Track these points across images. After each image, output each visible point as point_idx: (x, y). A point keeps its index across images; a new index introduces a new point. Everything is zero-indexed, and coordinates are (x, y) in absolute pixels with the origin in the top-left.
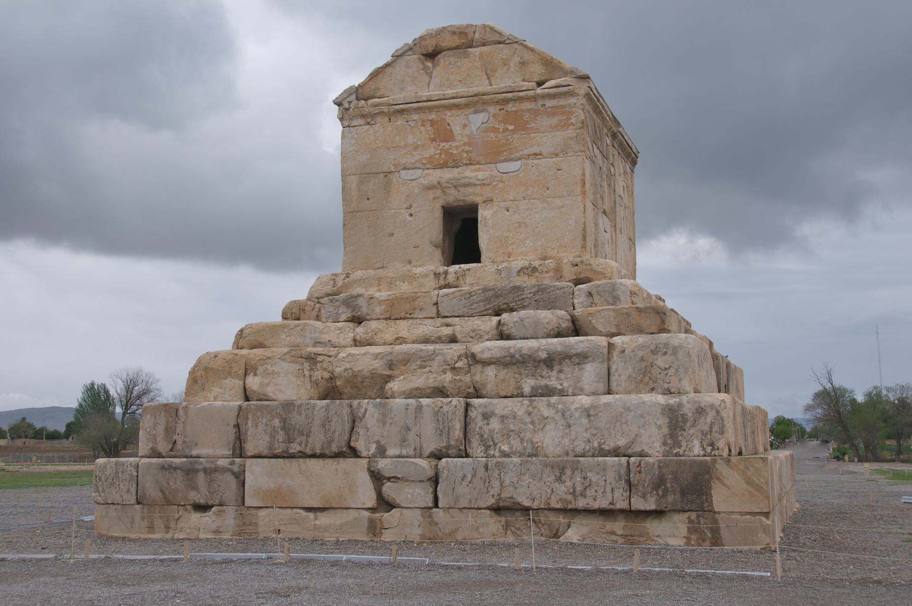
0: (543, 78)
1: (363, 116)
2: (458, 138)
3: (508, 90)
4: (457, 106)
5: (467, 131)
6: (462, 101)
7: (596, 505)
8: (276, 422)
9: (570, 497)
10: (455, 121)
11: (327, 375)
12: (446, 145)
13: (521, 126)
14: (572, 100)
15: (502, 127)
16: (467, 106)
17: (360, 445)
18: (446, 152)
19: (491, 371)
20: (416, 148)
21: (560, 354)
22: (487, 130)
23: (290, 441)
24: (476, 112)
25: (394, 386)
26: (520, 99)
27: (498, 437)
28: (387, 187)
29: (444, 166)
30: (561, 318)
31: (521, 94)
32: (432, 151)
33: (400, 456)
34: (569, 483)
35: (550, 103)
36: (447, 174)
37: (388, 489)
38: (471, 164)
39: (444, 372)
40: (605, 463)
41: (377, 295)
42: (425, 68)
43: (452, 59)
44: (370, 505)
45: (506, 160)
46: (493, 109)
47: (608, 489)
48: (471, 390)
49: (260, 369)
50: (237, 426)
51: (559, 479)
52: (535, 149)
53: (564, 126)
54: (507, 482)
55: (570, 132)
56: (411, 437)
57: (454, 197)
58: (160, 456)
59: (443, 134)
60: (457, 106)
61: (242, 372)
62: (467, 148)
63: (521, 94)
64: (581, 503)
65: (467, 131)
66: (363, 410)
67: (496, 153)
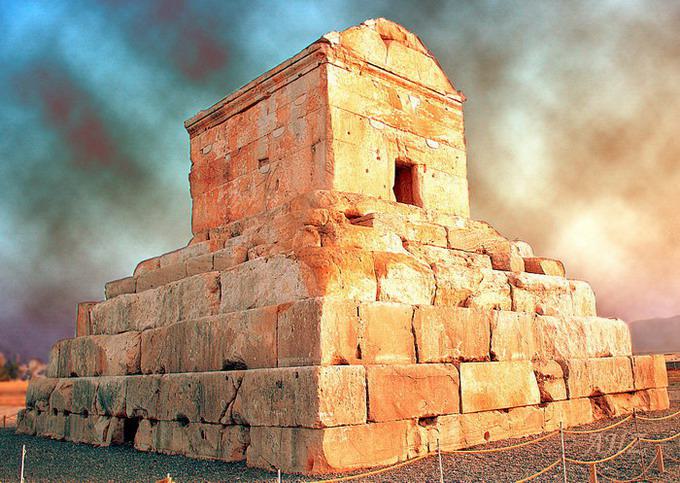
1: (345, 61)
9: (616, 384)
13: (437, 119)
16: (410, 88)
20: (380, 104)
27: (557, 345)
32: (388, 112)
35: (450, 109)
49: (390, 275)
50: (413, 331)
56: (523, 344)
57: (402, 155)
58: (343, 362)
59: (396, 104)
60: (404, 84)
65: (408, 106)
67: (426, 132)
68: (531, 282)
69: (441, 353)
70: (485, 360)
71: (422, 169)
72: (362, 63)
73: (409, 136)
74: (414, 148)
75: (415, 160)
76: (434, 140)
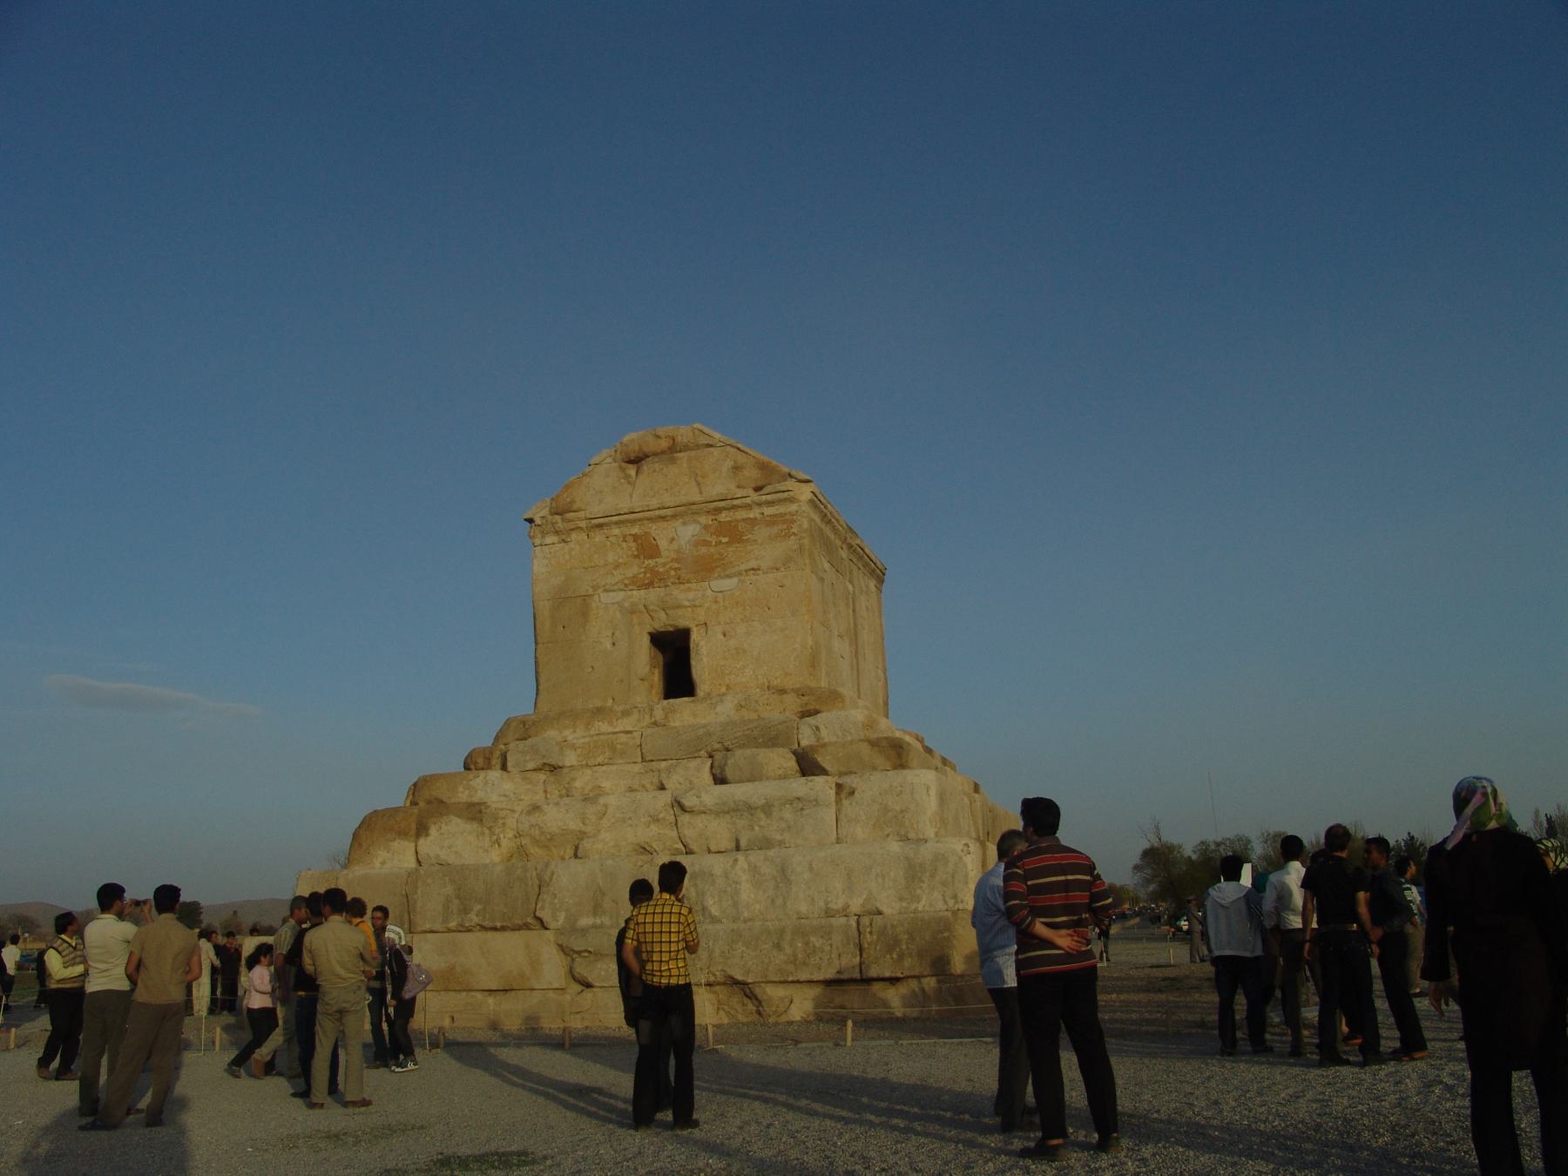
1: (557, 533)
2: (664, 553)
4: (663, 518)
5: (675, 546)
6: (668, 512)
8: (449, 889)
9: (791, 968)
10: (661, 534)
12: (651, 562)
14: (794, 507)
15: (713, 540)
16: (674, 516)
17: (545, 914)
18: (652, 570)
19: (700, 821)
20: (617, 567)
22: (697, 544)
23: (465, 910)
24: (684, 524)
26: (734, 507)
27: (710, 902)
28: (585, 613)
29: (650, 585)
31: (735, 502)
33: (594, 926)
34: (788, 950)
35: (768, 511)
36: (653, 595)
37: (581, 969)
41: (570, 738)
42: (627, 477)
43: (657, 466)
44: (556, 985)
45: (720, 577)
46: (703, 520)
47: (834, 955)
49: (433, 831)
52: (753, 564)
54: (717, 951)
55: (792, 542)
57: (663, 622)
59: (647, 549)
60: (663, 518)
61: (413, 832)
63: (735, 502)
64: (804, 977)
65: (675, 546)
66: (549, 873)
67: (706, 568)
69: (445, 921)
70: (527, 926)
71: (703, 631)
72: (583, 524)
74: (679, 607)
75: (682, 623)
76: (728, 576)
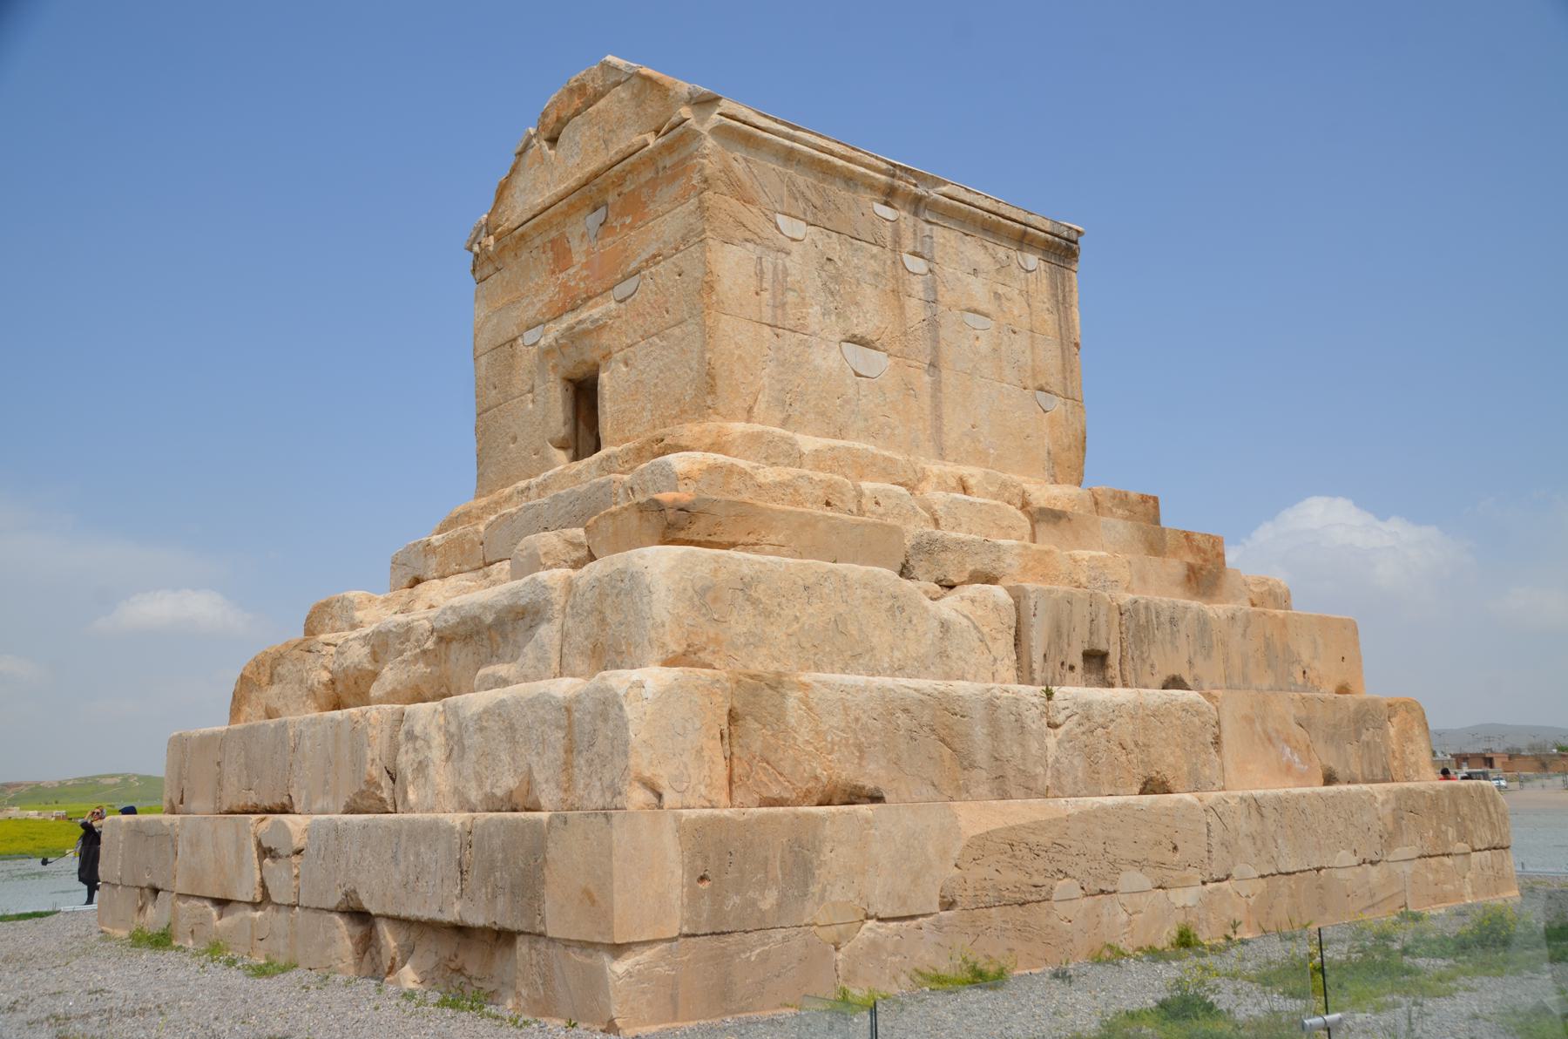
0: (661, 121)
3: (619, 157)
7: (426, 913)
11: (325, 676)
18: (564, 286)
21: (510, 609)
25: (375, 691)
30: (572, 544)
34: (402, 867)
38: (590, 298)
39: (416, 659)
40: (436, 823)
45: (625, 279)
48: (444, 690)
51: (394, 857)
52: (653, 250)
53: (685, 198)
62: (585, 273)
64: (413, 911)
68: (452, 619)
73: (584, 314)
